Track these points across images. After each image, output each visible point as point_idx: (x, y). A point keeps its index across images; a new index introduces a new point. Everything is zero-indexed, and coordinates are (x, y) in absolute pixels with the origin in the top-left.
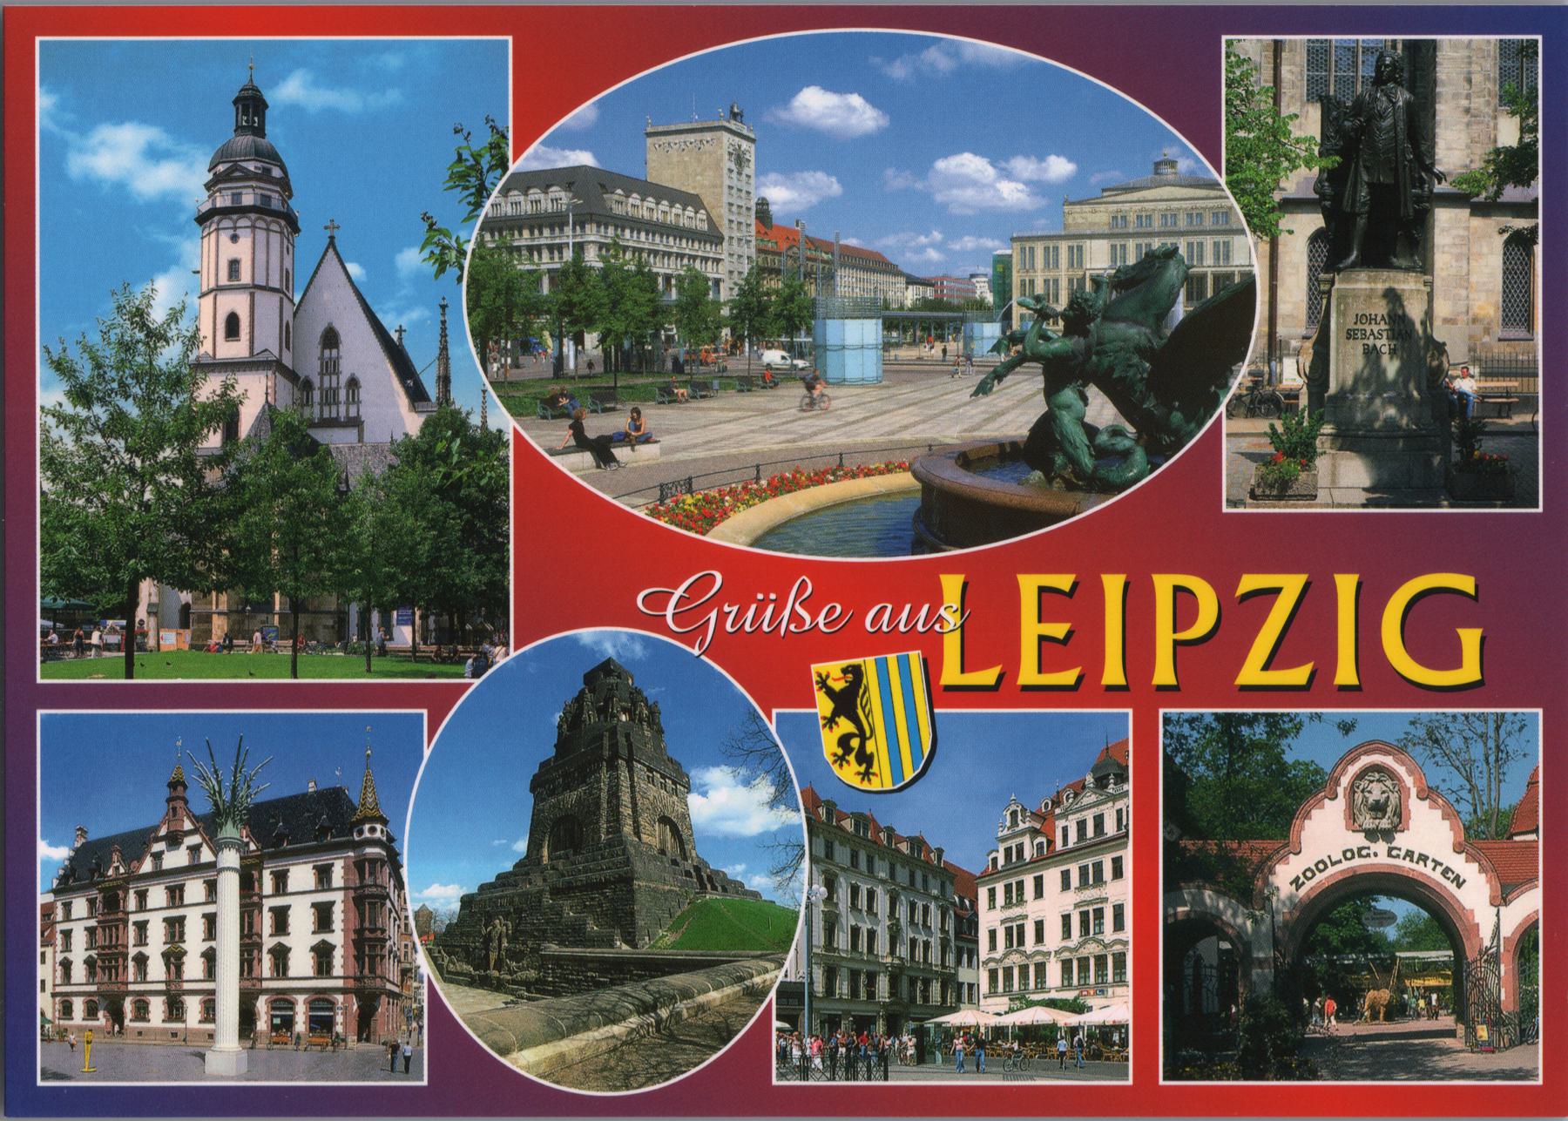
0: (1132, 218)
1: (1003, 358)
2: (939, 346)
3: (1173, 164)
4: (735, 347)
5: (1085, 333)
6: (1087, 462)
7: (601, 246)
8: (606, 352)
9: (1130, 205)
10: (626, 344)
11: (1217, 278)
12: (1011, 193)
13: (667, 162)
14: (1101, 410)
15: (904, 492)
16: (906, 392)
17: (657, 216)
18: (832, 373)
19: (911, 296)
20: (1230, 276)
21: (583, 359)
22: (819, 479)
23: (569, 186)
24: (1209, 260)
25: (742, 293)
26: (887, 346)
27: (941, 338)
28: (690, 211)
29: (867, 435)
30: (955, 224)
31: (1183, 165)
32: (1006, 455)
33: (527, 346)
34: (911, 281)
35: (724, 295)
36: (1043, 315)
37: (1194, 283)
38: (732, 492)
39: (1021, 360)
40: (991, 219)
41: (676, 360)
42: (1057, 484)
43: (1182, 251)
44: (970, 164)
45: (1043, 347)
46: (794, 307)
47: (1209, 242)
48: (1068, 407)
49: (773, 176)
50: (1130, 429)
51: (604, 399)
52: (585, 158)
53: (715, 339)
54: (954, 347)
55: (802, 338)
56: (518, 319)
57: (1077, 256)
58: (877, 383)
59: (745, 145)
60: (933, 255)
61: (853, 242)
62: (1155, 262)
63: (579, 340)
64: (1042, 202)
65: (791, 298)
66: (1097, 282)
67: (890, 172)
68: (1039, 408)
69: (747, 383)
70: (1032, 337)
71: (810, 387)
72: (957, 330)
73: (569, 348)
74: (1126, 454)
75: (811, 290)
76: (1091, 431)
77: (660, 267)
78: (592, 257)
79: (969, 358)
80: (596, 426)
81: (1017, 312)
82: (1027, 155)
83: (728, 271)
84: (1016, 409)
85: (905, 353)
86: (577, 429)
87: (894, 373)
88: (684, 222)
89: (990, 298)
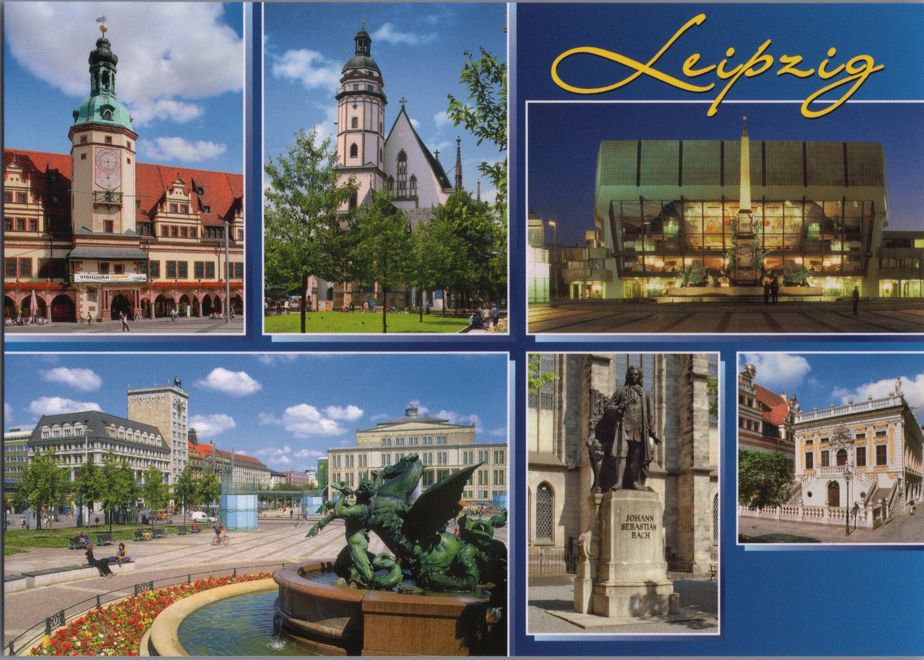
0: (393, 440)
1: (323, 516)
2: (288, 510)
3: (415, 410)
4: (177, 511)
5: (368, 503)
6: (369, 573)
7: (104, 455)
8: (106, 513)
9: (393, 433)
10: (117, 509)
11: (439, 472)
12: (328, 426)
13: (140, 409)
14: (377, 545)
15: (270, 589)
16: (273, 535)
17: (134, 439)
18: (230, 524)
19: (273, 482)
20: (447, 471)
21: (93, 517)
22: (223, 582)
23: (86, 422)
24: (435, 462)
25: (181, 481)
26: (260, 510)
27: (290, 505)
28: (152, 436)
29: (249, 558)
30: (297, 443)
31: (422, 411)
32: (325, 569)
33: (62, 510)
34: (274, 474)
35: (171, 482)
36: (345, 493)
37: (427, 475)
38: (175, 589)
39: (333, 517)
40: (317, 440)
41: (144, 517)
42: (353, 585)
43: (421, 458)
44: (306, 410)
45: (345, 511)
46: (209, 489)
47: (435, 453)
48: (358, 543)
49: (198, 417)
50: (392, 555)
51: (105, 539)
52: (94, 407)
53: (166, 506)
54: (297, 510)
55: (214, 505)
56: (58, 494)
57: (363, 461)
58: (254, 530)
59: (182, 400)
60: (285, 460)
61: (241, 453)
62: (405, 464)
63: (91, 506)
64: (344, 431)
65: (207, 484)
66: (374, 475)
67: (262, 415)
68: (342, 543)
69: (182, 530)
70: (339, 504)
71: (218, 532)
72: (299, 501)
73: (85, 510)
74: (390, 569)
75: (219, 479)
76: (371, 556)
77: (135, 466)
78: (98, 461)
79: (305, 517)
80: (100, 553)
81: (331, 491)
82: (336, 405)
83: (173, 469)
84: (330, 544)
85: (270, 514)
86: (90, 555)
87: (264, 524)
88: (148, 442)
89: (316, 483)
